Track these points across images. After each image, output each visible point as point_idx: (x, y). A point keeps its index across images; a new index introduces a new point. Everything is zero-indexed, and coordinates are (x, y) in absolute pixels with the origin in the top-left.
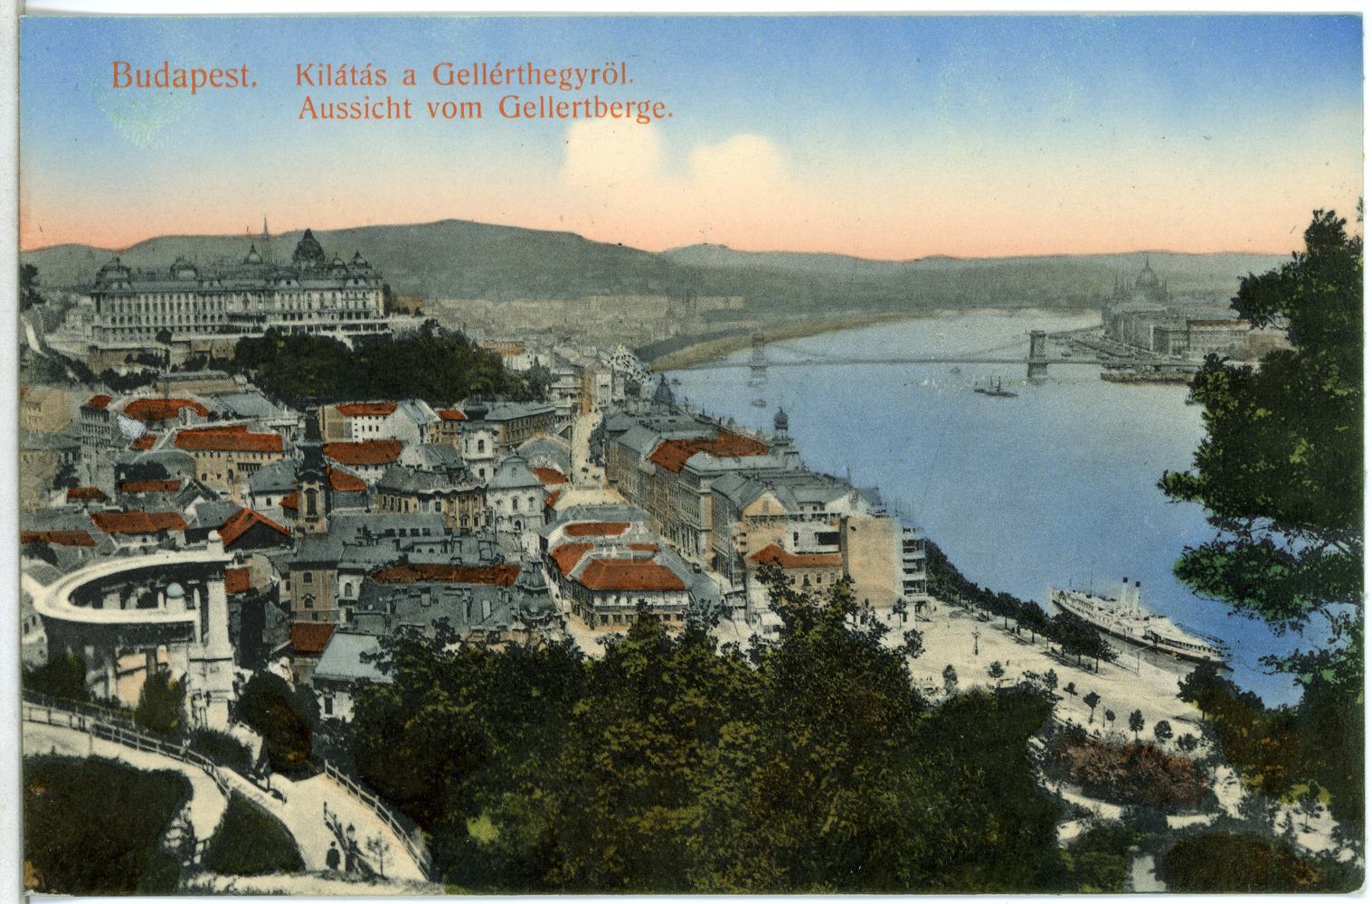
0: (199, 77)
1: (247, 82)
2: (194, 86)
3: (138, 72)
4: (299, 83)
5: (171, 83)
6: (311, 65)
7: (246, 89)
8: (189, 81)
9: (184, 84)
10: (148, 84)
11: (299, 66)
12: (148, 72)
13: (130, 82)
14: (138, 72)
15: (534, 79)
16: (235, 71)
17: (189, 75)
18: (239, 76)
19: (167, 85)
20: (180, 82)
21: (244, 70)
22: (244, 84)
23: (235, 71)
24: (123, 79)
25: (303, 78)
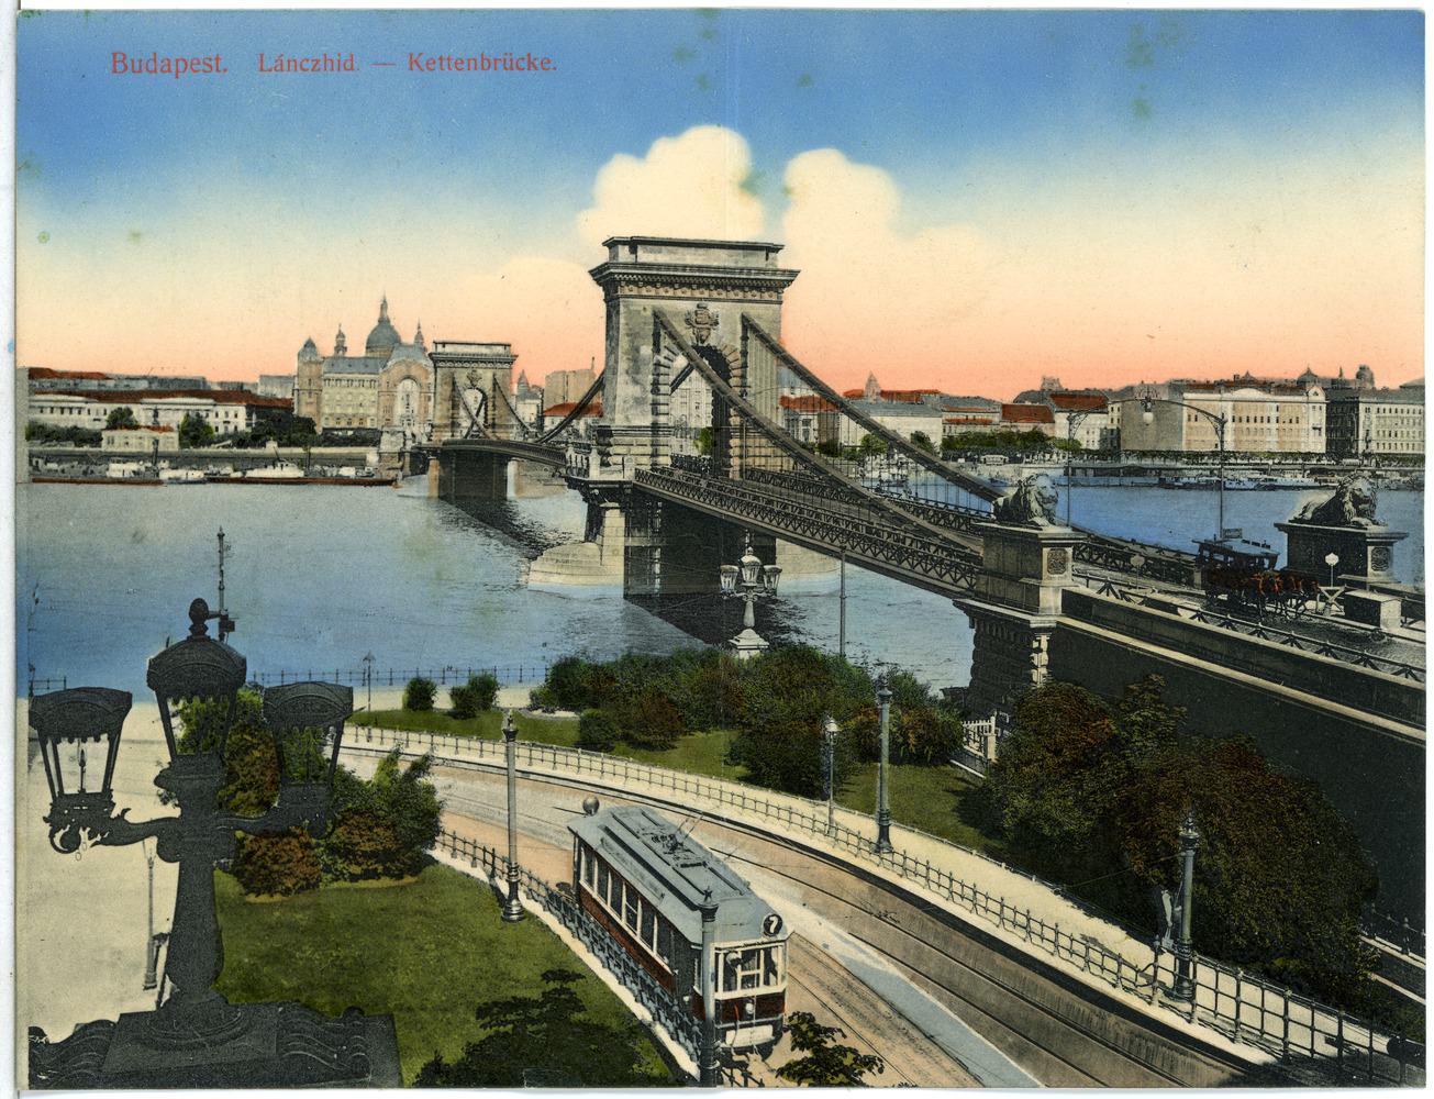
0: (181, 64)
1: (220, 68)
2: (177, 71)
3: (133, 61)
4: (412, 69)
5: (159, 70)
6: (421, 54)
7: (221, 73)
8: (173, 68)
9: (169, 71)
10: (140, 71)
11: (411, 55)
12: (140, 61)
13: (126, 67)
14: (133, 61)
15: (329, 67)
16: (210, 59)
17: (173, 63)
18: (213, 63)
19: (155, 71)
20: (166, 68)
21: (217, 59)
22: (218, 70)
23: (210, 59)
24: (120, 67)
25: (415, 66)
